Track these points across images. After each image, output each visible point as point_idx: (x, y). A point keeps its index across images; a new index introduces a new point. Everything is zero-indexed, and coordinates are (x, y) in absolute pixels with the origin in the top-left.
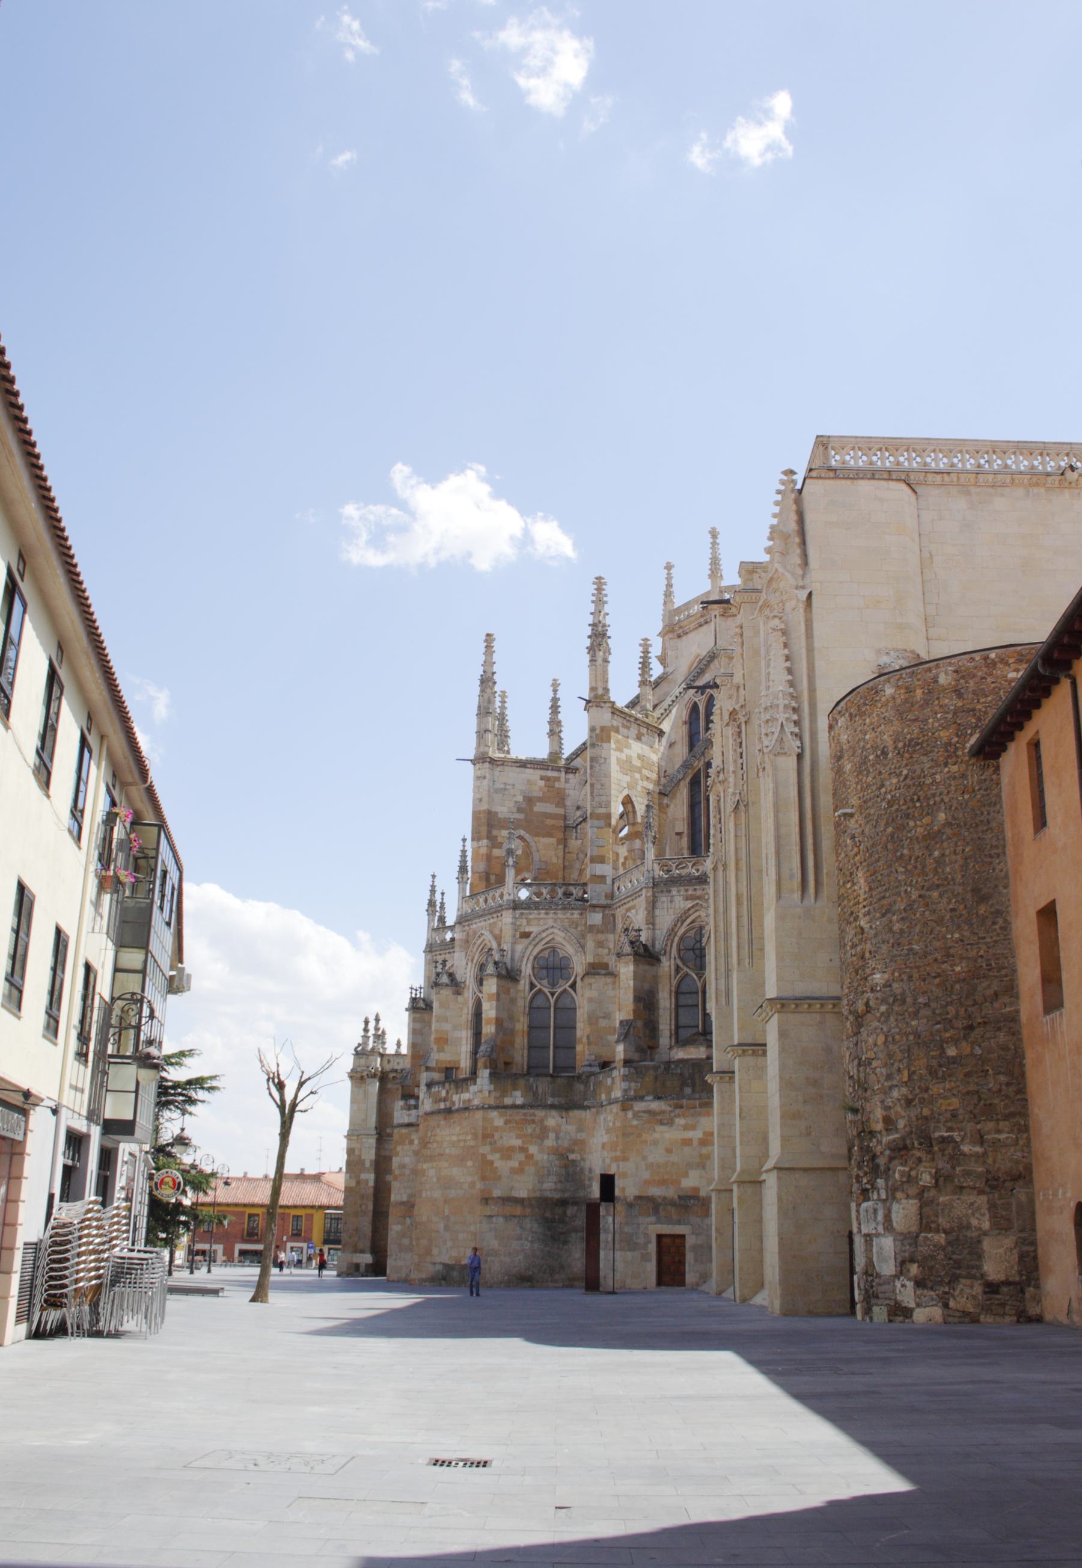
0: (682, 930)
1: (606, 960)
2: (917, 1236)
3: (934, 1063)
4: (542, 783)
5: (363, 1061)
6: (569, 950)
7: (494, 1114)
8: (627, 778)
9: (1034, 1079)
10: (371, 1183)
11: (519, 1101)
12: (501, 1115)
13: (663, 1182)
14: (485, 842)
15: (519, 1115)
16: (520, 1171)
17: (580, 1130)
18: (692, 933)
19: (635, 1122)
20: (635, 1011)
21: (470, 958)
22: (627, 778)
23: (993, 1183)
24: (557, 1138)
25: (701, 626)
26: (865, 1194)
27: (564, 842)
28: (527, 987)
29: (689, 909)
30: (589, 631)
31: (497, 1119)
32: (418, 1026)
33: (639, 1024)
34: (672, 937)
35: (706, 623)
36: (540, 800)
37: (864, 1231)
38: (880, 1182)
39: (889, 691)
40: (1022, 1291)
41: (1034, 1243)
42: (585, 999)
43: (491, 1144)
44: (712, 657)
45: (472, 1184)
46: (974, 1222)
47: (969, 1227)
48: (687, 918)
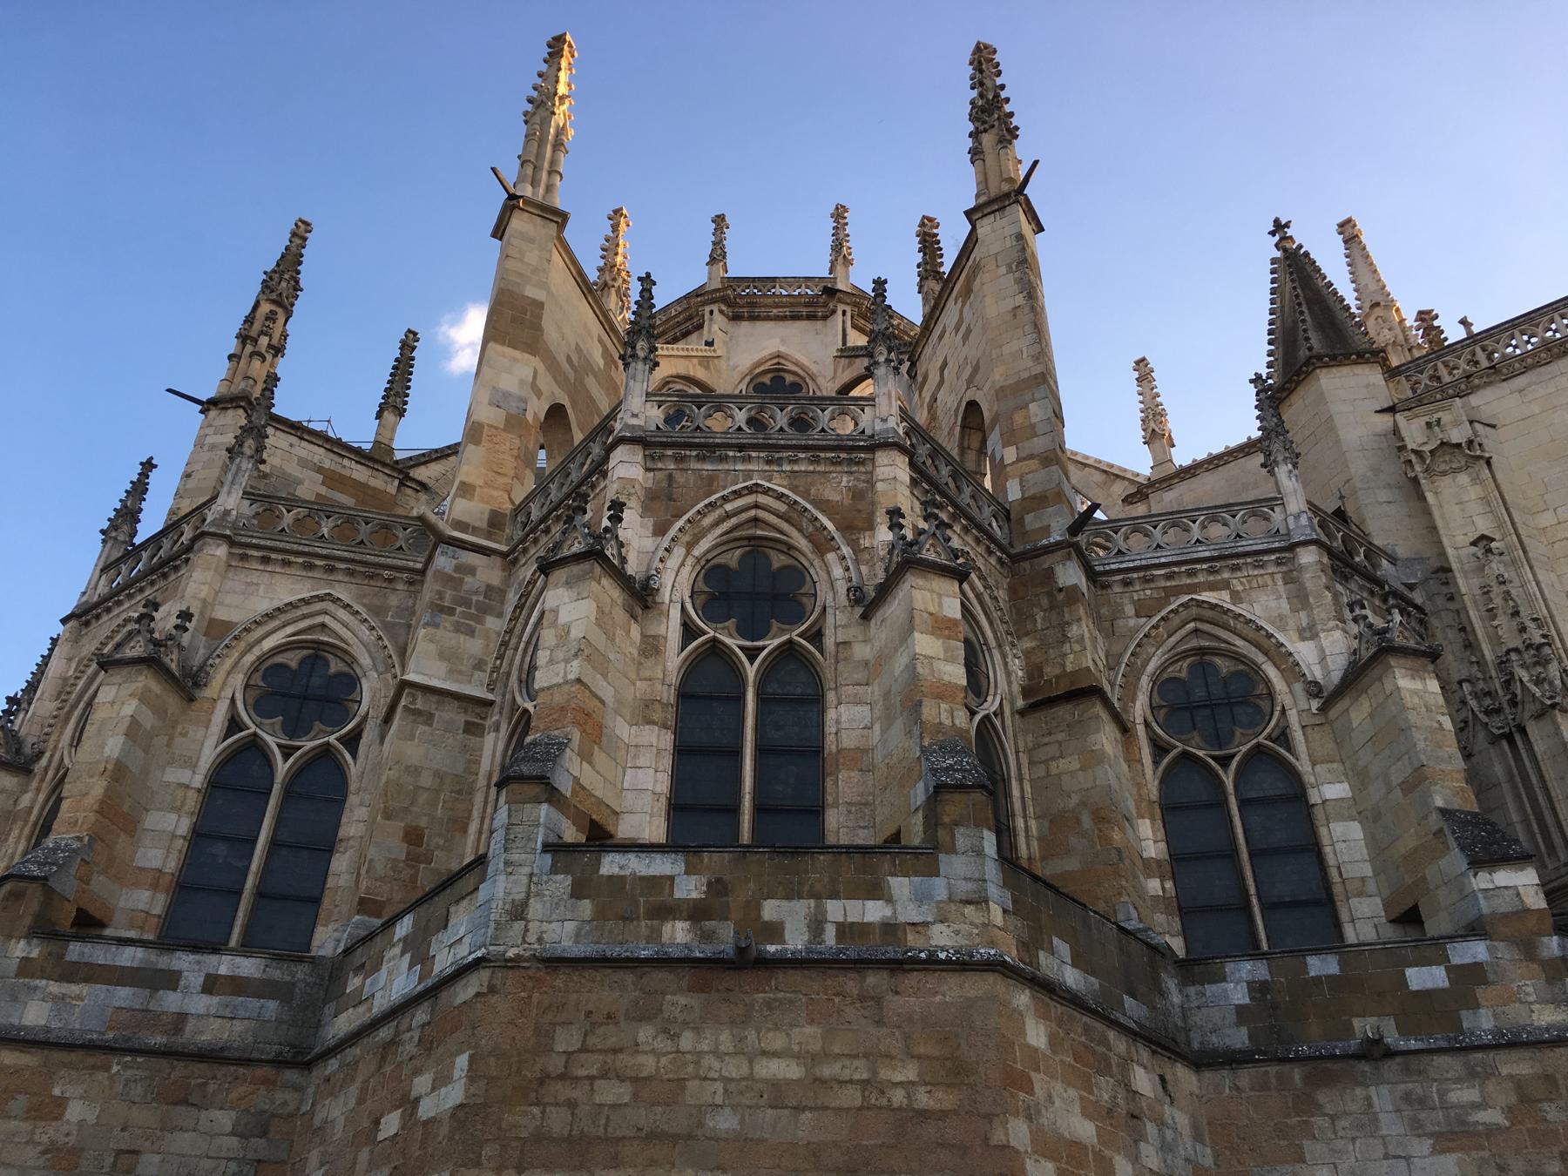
7: (1023, 999)
12: (1043, 1015)
21: (687, 538)
25: (795, 317)
35: (811, 317)
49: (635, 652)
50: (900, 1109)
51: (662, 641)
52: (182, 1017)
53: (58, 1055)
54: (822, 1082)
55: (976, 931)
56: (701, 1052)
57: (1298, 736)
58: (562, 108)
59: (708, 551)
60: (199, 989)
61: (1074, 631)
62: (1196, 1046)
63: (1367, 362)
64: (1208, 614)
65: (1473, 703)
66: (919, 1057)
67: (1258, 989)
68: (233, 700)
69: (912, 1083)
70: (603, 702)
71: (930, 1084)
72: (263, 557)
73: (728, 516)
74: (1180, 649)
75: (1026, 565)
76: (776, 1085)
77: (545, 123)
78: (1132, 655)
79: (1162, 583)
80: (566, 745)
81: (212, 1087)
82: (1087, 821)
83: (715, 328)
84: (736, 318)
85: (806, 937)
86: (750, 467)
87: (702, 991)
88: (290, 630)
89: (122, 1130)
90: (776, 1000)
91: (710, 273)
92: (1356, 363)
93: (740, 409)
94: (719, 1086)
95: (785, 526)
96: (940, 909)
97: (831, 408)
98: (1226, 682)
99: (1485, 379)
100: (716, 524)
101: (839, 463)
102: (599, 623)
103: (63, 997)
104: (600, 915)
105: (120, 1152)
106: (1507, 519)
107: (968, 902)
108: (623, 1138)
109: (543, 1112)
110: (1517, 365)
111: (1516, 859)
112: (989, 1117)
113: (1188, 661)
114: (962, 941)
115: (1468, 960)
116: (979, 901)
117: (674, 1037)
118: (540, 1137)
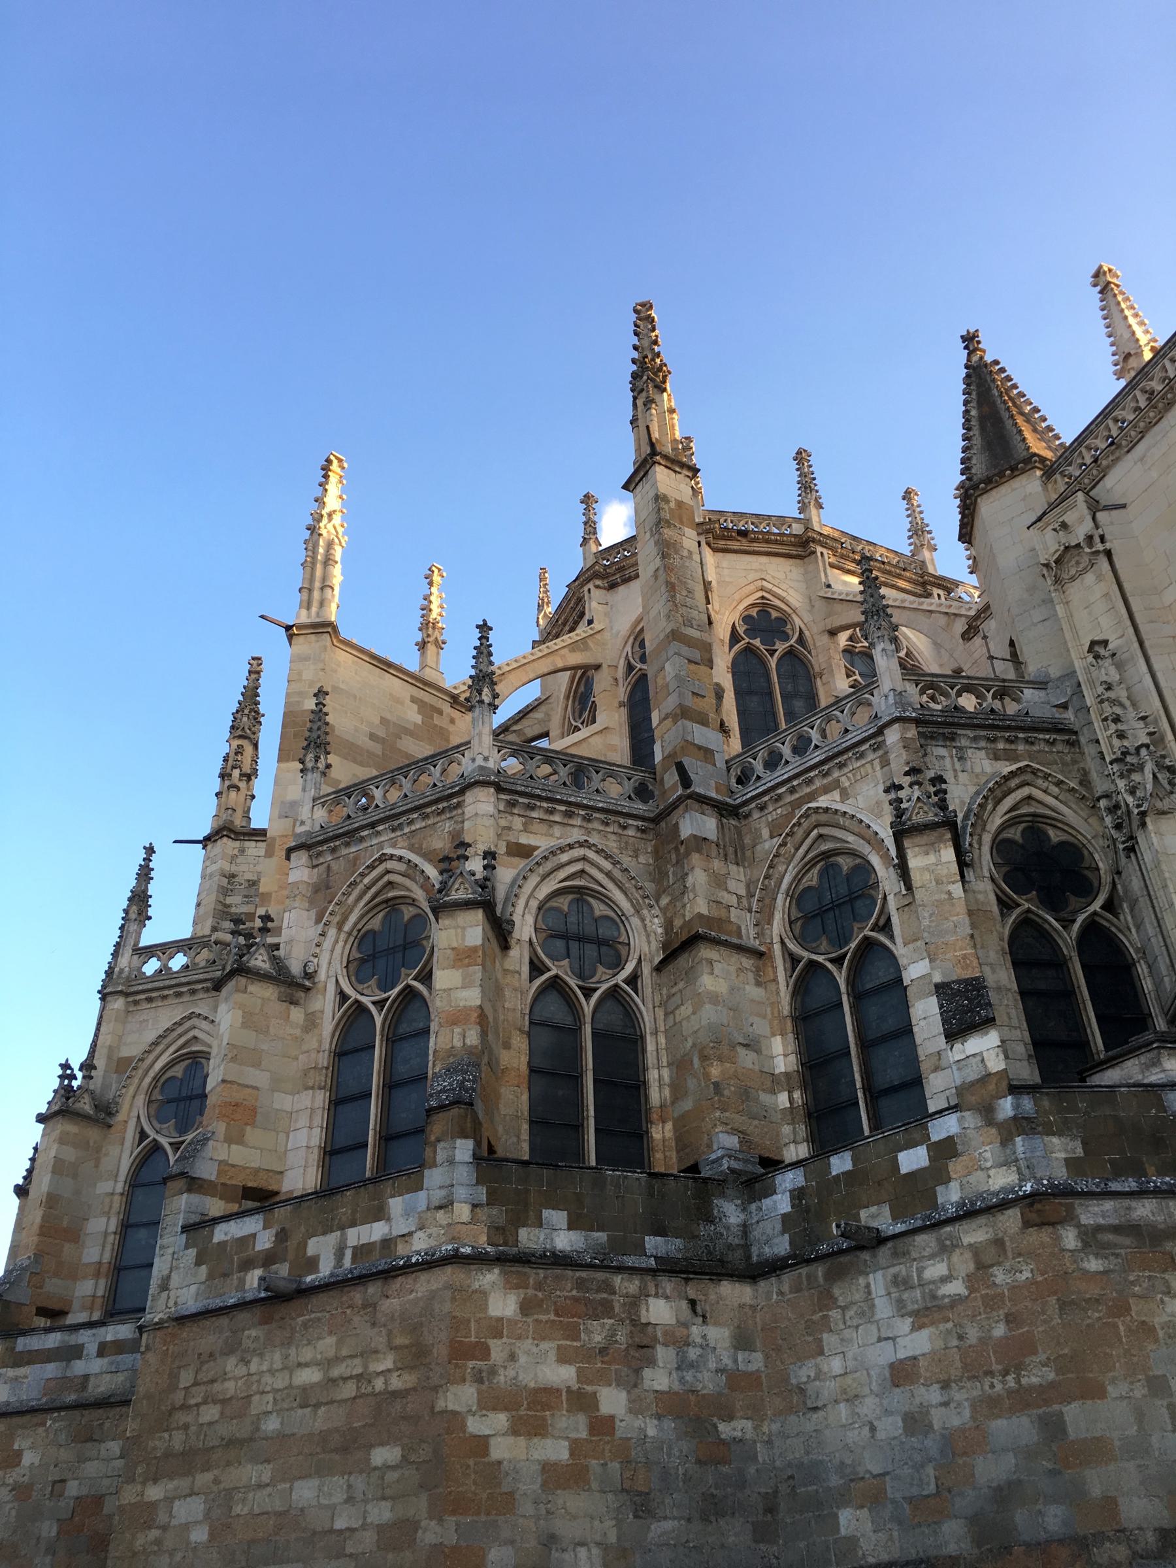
0: (997, 821)
7: (490, 1278)
12: (510, 1286)
15: (566, 1286)
18: (1015, 833)
19: (1094, 1265)
21: (337, 919)
24: (683, 1365)
28: (526, 969)
29: (1006, 778)
32: (70, 1154)
34: (978, 830)
43: (479, 1379)
48: (1006, 795)
49: (298, 1032)
50: (380, 1393)
51: (319, 1014)
52: (86, 1377)
53: (16, 1420)
54: (333, 1381)
55: (442, 1232)
56: (263, 1372)
57: (895, 920)
58: (330, 526)
59: (356, 924)
60: (95, 1355)
61: (690, 881)
62: (755, 1259)
63: (1024, 472)
64: (823, 818)
65: (1108, 820)
66: (396, 1348)
67: (798, 1195)
68: (139, 1117)
69: (389, 1371)
70: (256, 1088)
71: (401, 1369)
72: (146, 999)
73: (368, 888)
74: (806, 860)
75: (663, 824)
76: (305, 1389)
77: (316, 545)
78: (765, 878)
79: (789, 798)
80: (208, 1139)
81: (107, 1425)
82: (696, 1062)
83: (594, 604)
84: (612, 586)
85: (332, 1264)
86: (382, 839)
87: (266, 1323)
88: (172, 1049)
89: (55, 1466)
90: (309, 1320)
91: (584, 554)
92: (1013, 477)
93: (377, 787)
94: (270, 1397)
95: (407, 882)
96: (420, 1218)
97: (441, 761)
98: (848, 877)
99: (1111, 458)
100: (360, 897)
101: (443, 811)
102: (245, 1025)
103: (16, 1378)
104: (211, 1276)
105: (55, 1482)
106: (1124, 611)
107: (440, 1207)
108: (213, 1447)
109: (170, 1435)
110: (1133, 433)
111: (980, 1025)
112: (436, 1389)
113: (818, 867)
114: (433, 1243)
115: (943, 1135)
116: (446, 1205)
117: (247, 1363)
118: (168, 1454)
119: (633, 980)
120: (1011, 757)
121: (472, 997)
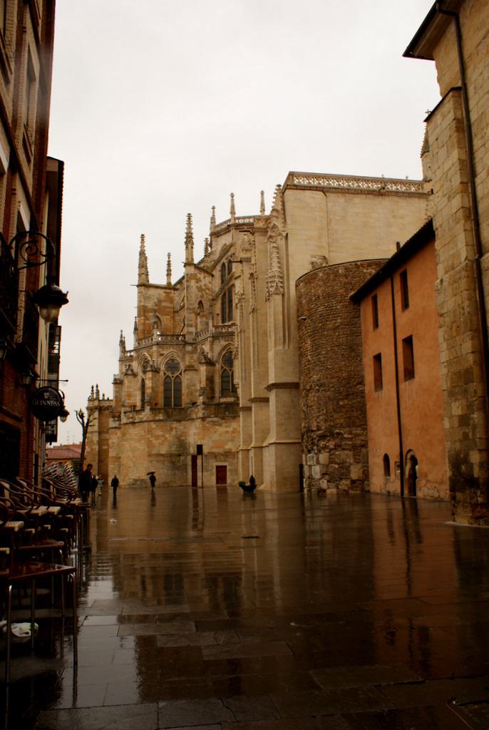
1: (194, 364)
2: (328, 466)
3: (335, 408)
4: (164, 294)
5: (92, 403)
6: (179, 360)
7: (152, 423)
8: (200, 294)
9: (370, 413)
10: (97, 450)
11: (161, 418)
13: (219, 447)
14: (143, 318)
15: (162, 424)
16: (162, 444)
17: (185, 428)
18: (227, 354)
20: (206, 384)
22: (200, 294)
23: (354, 448)
24: (176, 431)
25: (226, 233)
26: (309, 452)
27: (173, 317)
30: (185, 236)
31: (153, 425)
33: (208, 388)
36: (164, 301)
37: (309, 464)
38: (315, 447)
39: (321, 274)
40: (363, 483)
41: (367, 467)
42: (186, 379)
44: (231, 246)
45: (144, 449)
46: (348, 460)
47: (346, 462)
84: (218, 237)
119: (180, 374)
120: (228, 341)
121: (150, 385)
